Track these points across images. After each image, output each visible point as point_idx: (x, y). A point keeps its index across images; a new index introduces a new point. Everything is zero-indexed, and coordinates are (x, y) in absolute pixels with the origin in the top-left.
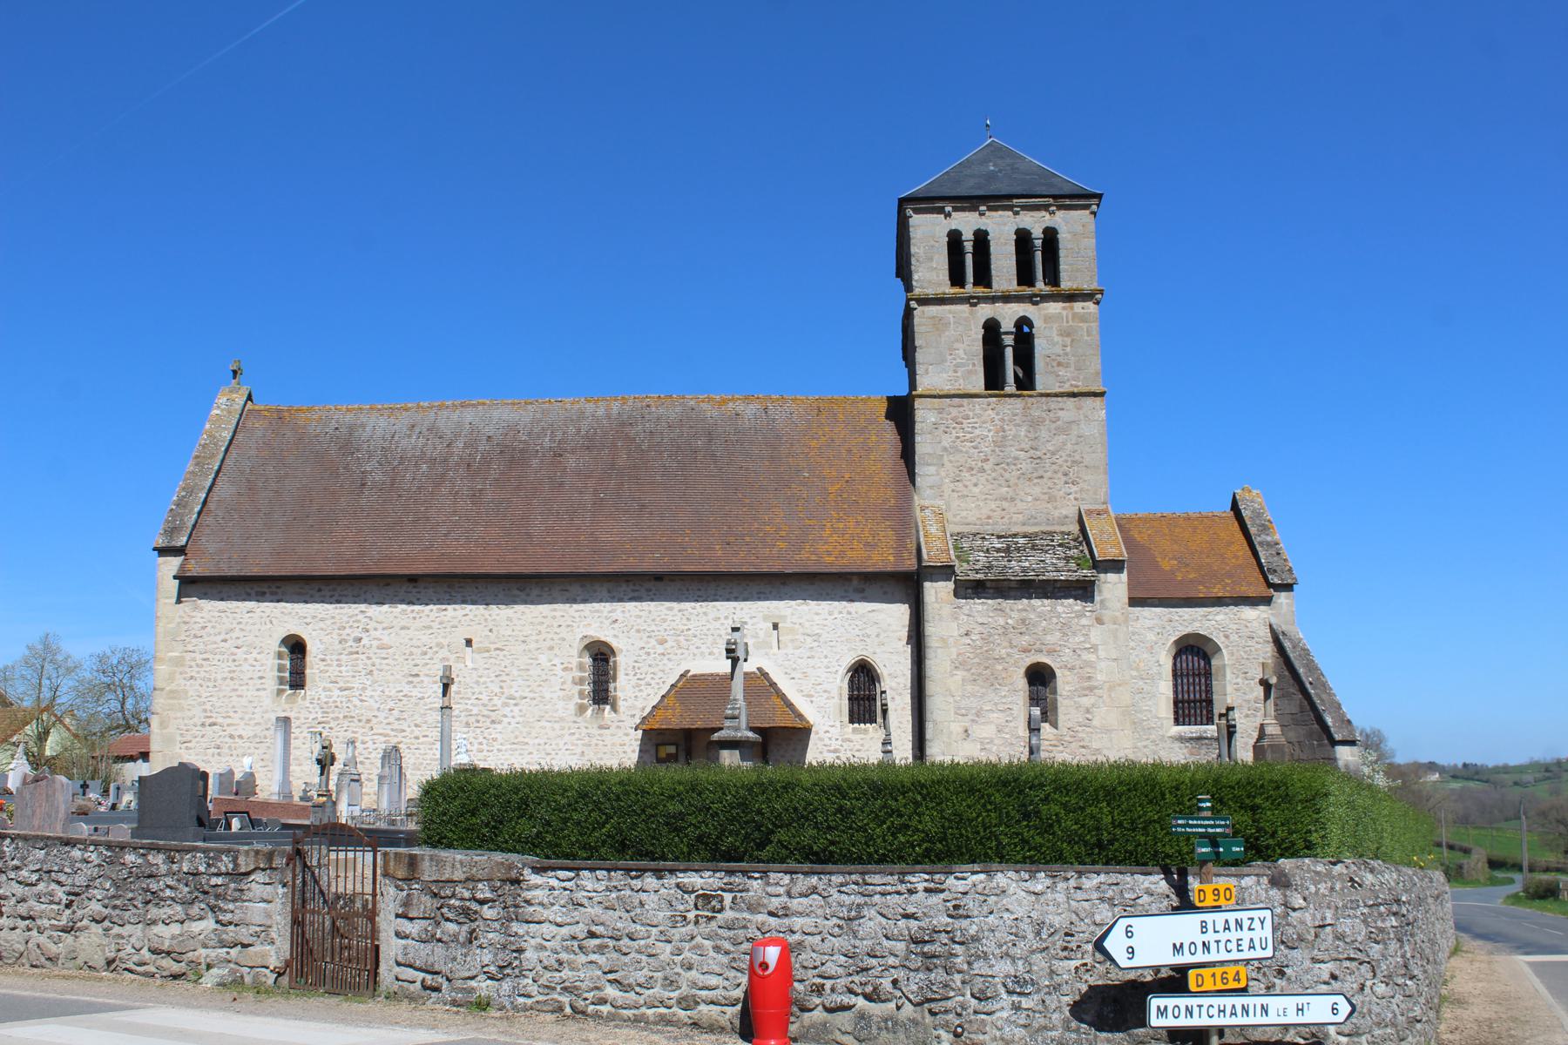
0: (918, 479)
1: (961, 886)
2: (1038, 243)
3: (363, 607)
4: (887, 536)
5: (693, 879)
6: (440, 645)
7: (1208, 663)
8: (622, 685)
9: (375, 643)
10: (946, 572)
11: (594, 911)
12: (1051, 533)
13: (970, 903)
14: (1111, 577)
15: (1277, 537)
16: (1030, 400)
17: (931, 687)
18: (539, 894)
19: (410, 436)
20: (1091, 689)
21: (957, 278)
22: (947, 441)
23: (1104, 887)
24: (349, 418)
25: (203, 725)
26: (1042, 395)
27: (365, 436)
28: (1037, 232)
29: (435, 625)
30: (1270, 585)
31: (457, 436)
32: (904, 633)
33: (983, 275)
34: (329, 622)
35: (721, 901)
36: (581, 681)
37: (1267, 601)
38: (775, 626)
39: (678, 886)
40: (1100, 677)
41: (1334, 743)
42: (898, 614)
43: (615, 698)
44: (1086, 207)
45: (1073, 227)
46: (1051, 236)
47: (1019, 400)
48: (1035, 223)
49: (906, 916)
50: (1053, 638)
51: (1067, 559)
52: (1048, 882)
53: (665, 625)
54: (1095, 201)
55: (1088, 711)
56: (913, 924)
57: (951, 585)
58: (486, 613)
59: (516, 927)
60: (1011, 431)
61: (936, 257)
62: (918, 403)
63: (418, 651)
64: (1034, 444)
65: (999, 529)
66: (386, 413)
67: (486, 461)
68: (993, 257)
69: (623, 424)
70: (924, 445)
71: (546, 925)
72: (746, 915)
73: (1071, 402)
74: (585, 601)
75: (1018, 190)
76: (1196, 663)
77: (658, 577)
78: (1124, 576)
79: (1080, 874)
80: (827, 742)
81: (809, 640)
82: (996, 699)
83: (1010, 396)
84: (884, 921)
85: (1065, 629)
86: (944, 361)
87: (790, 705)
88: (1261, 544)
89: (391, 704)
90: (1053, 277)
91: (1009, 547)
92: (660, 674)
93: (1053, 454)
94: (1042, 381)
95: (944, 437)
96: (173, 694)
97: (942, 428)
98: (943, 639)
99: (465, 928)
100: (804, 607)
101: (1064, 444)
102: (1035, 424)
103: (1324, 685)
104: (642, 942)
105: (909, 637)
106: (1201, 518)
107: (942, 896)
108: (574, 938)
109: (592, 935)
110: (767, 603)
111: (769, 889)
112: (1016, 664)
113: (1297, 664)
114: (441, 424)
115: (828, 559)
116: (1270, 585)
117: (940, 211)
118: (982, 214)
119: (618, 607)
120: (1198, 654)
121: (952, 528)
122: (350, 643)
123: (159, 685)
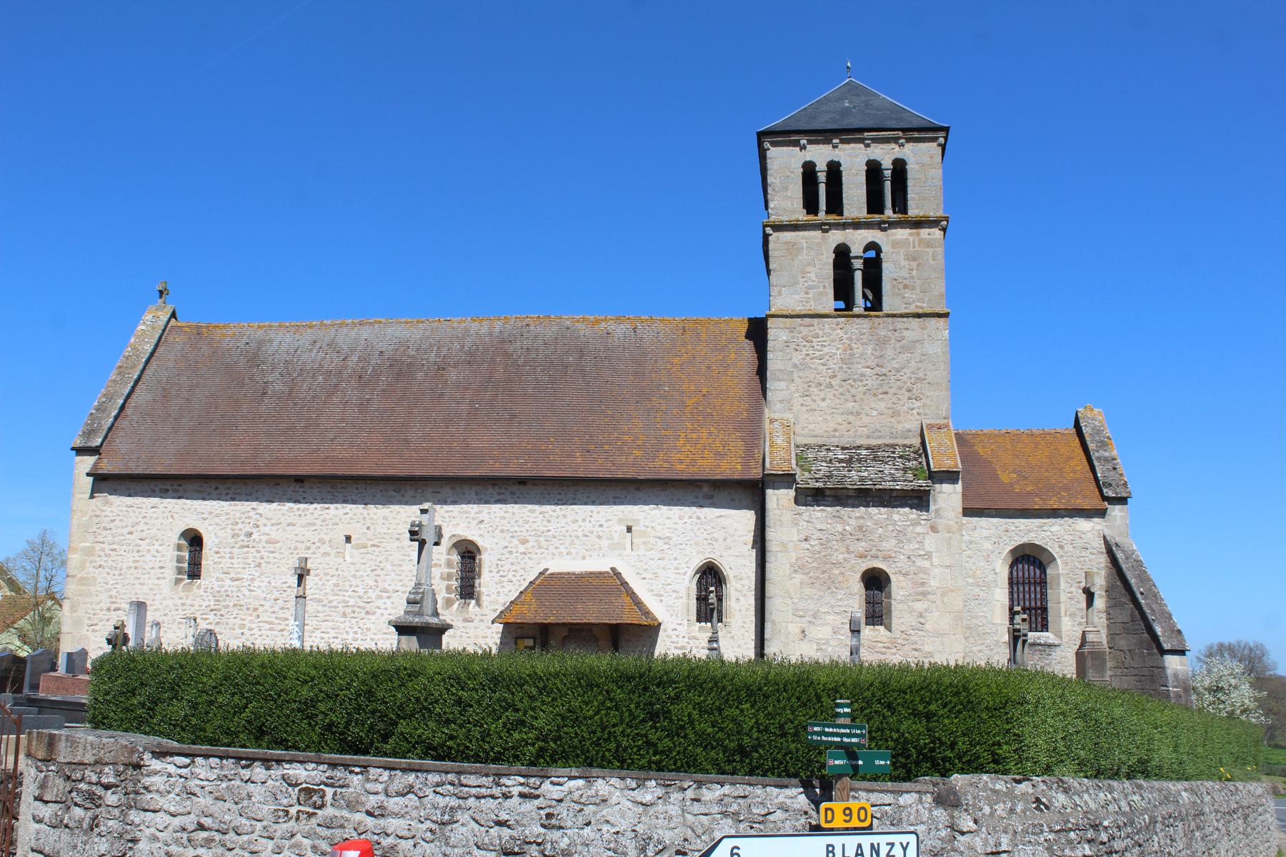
0: (769, 394)
1: (556, 792)
2: (888, 173)
3: (254, 504)
4: (737, 447)
5: (299, 772)
6: (322, 541)
8: (487, 582)
10: (787, 480)
12: (893, 446)
13: (562, 810)
14: (946, 487)
15: (1115, 453)
18: (157, 781)
19: (311, 351)
21: (810, 204)
22: (797, 358)
24: (260, 333)
25: (109, 609)
26: (888, 316)
27: (271, 350)
28: (887, 164)
30: (1105, 498)
31: (352, 351)
33: (835, 205)
34: (223, 518)
35: (323, 797)
36: (449, 577)
37: (1102, 513)
38: (629, 529)
41: (1163, 652)
42: (746, 518)
45: (922, 159)
46: (900, 168)
48: (885, 155)
49: (500, 823)
51: (905, 470)
52: (660, 792)
53: (527, 527)
55: (921, 615)
56: (506, 832)
57: (792, 493)
58: (365, 512)
59: (134, 816)
61: (791, 186)
62: (771, 323)
63: (303, 546)
64: (880, 361)
65: (845, 441)
66: (293, 330)
67: (376, 374)
68: (844, 187)
69: (503, 341)
71: (161, 814)
72: (346, 813)
74: (454, 502)
76: (1035, 572)
77: (522, 481)
79: (700, 784)
81: (660, 543)
84: (476, 826)
85: (900, 535)
86: (796, 283)
87: (638, 603)
88: (1099, 459)
89: (276, 594)
90: (901, 203)
91: (851, 458)
92: (521, 572)
94: (888, 304)
96: (83, 581)
97: (793, 346)
98: (784, 545)
99: (90, 814)
102: (881, 343)
103: (1156, 596)
104: (245, 838)
105: (755, 542)
106: (1045, 435)
107: (536, 802)
109: (201, 827)
110: (622, 507)
111: (369, 786)
113: (1129, 575)
114: (340, 340)
116: (1105, 498)
117: (796, 144)
118: (835, 147)
120: (1033, 564)
121: (802, 440)
122: (242, 537)
123: (71, 572)
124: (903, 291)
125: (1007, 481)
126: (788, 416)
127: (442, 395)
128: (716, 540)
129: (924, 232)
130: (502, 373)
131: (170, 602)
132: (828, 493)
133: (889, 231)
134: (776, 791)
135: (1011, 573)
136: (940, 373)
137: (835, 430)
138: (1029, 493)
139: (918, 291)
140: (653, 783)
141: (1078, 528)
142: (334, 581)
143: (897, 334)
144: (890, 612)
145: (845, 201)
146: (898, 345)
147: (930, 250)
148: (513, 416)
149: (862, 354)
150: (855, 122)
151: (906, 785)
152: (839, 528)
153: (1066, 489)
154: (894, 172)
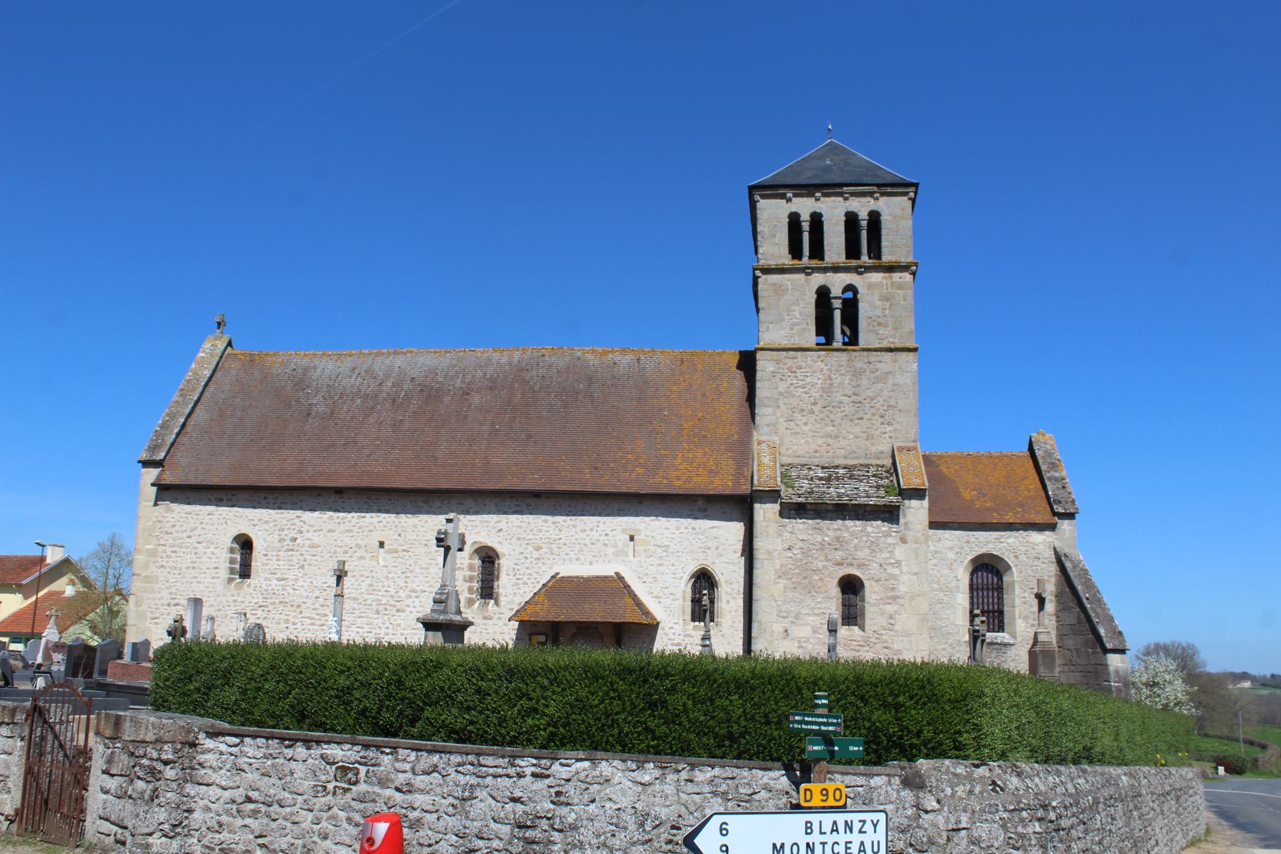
0: (757, 419)
2: (864, 223)
3: (299, 513)
4: (728, 465)
5: (335, 752)
6: (359, 546)
7: (1001, 579)
8: (504, 584)
9: (307, 543)
10: (772, 495)
11: (251, 776)
12: (867, 466)
13: (570, 789)
14: (914, 503)
15: (1064, 473)
18: (210, 758)
19: (350, 377)
21: (795, 251)
22: (782, 387)
23: (717, 781)
25: (169, 605)
26: (864, 350)
28: (863, 215)
29: (355, 529)
30: (1055, 514)
31: (387, 377)
32: (739, 547)
33: (818, 250)
35: (357, 774)
36: (471, 579)
37: (1052, 527)
38: (632, 538)
39: (322, 756)
42: (735, 530)
43: (498, 594)
44: (905, 194)
45: (894, 210)
46: (875, 218)
48: (862, 206)
49: (515, 800)
51: (878, 487)
52: (657, 773)
54: (912, 189)
55: (891, 617)
57: (777, 507)
58: (397, 521)
59: (190, 789)
60: (837, 379)
61: (778, 235)
62: (759, 355)
64: (856, 390)
65: (825, 462)
67: (408, 398)
69: (521, 370)
70: (763, 390)
72: (377, 789)
73: (887, 356)
74: (476, 513)
75: (848, 180)
77: (537, 495)
78: (926, 503)
79: (693, 766)
80: (671, 636)
81: (659, 550)
84: (493, 802)
85: (874, 546)
86: (783, 320)
87: (639, 604)
88: (1050, 479)
89: (317, 593)
90: (875, 250)
91: (830, 476)
92: (535, 575)
93: (872, 399)
94: (865, 339)
95: (781, 383)
96: (148, 579)
97: (779, 376)
98: (769, 553)
99: (151, 786)
100: (656, 523)
101: (881, 391)
102: (858, 374)
103: (1100, 601)
104: (288, 810)
105: (743, 550)
106: (1002, 457)
107: (547, 781)
108: (234, 802)
109: (249, 800)
110: (625, 519)
111: (398, 765)
114: (376, 367)
116: (1055, 514)
117: (783, 196)
118: (817, 200)
119: (503, 518)
120: (992, 571)
121: (786, 460)
123: (137, 572)
126: (776, 438)
127: (466, 417)
129: (896, 276)
130: (518, 397)
131: (222, 599)
132: (809, 507)
134: (761, 773)
135: (971, 580)
136: (909, 401)
138: (987, 509)
140: (652, 765)
141: (1031, 540)
142: (369, 581)
144: (863, 614)
145: (826, 248)
146: (873, 376)
148: (529, 437)
149: (840, 384)
151: (877, 769)
152: (819, 538)
153: (1021, 505)
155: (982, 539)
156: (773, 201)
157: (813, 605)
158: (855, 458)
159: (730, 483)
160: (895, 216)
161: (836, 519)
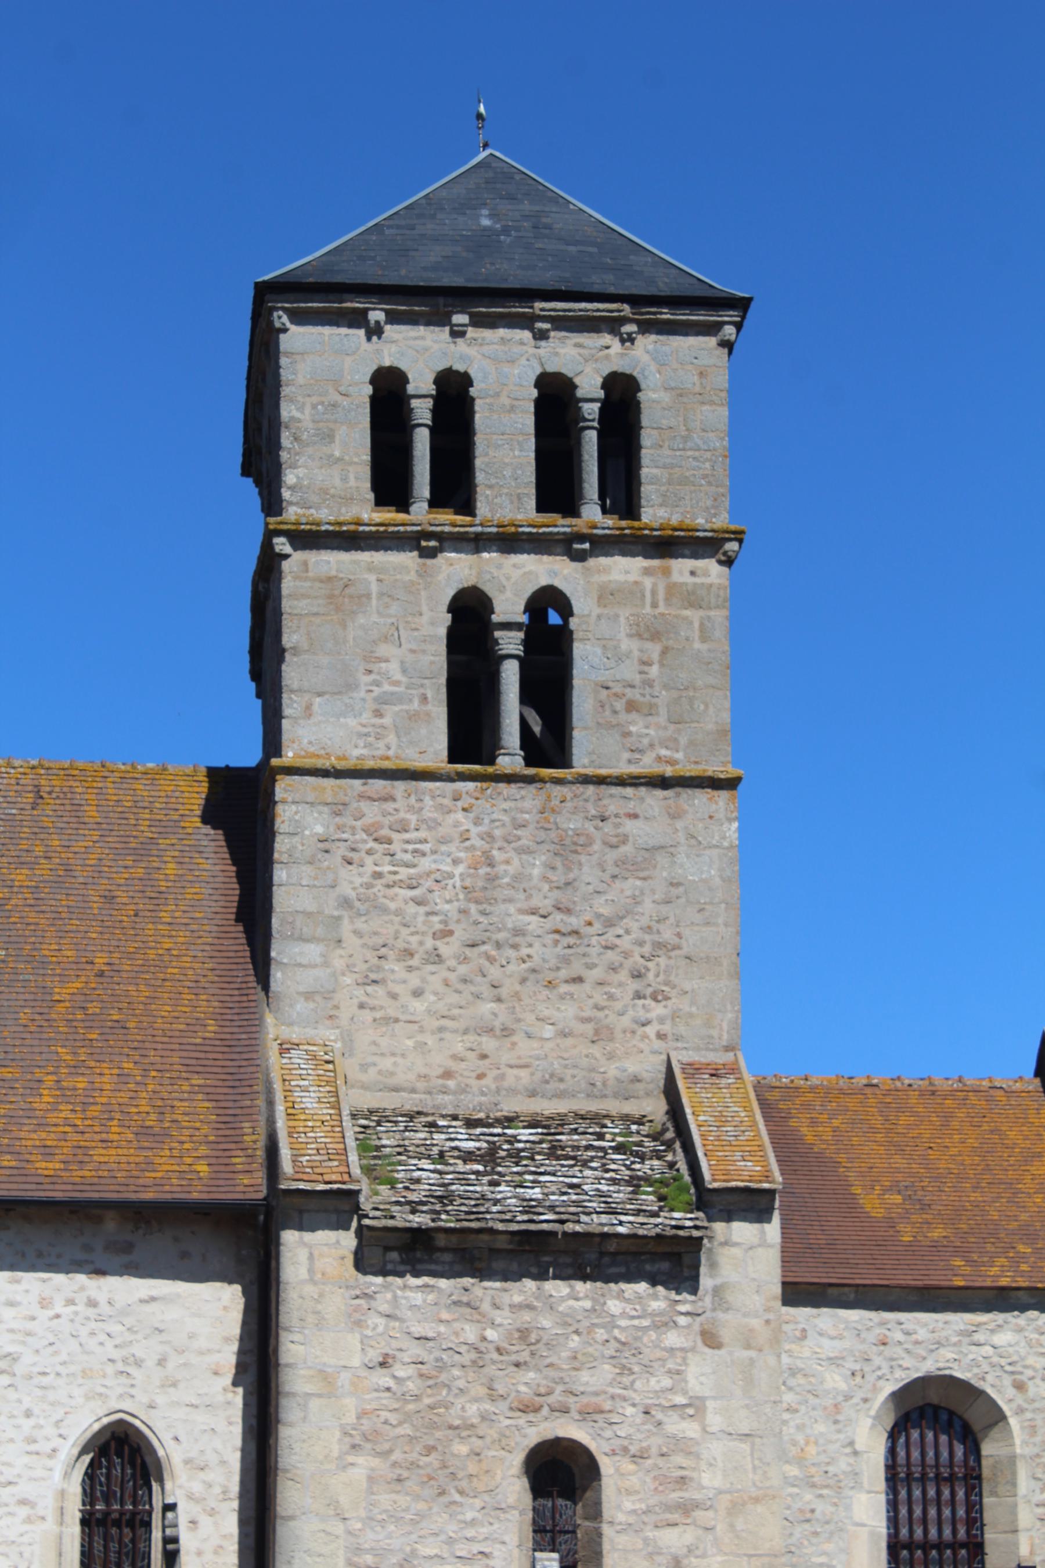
0: (277, 976)
2: (591, 410)
7: (974, 1449)
10: (336, 1206)
12: (597, 1118)
14: (742, 1230)
16: (557, 791)
17: (292, 1497)
20: (687, 1508)
21: (390, 484)
26: (586, 780)
28: (589, 385)
32: (228, 1357)
33: (455, 486)
40: (710, 1480)
45: (677, 374)
46: (622, 395)
47: (532, 789)
48: (586, 361)
50: (596, 1379)
51: (635, 1182)
54: (731, 316)
57: (347, 1240)
61: (341, 432)
62: (284, 788)
65: (472, 1104)
70: (292, 891)
73: (654, 799)
76: (950, 1451)
78: (773, 1229)
82: (451, 1529)
83: (510, 779)
85: (626, 1355)
86: (351, 686)
90: (623, 492)
91: (493, 1148)
93: (609, 923)
94: (588, 747)
98: (326, 1377)
101: (636, 900)
102: (567, 850)
106: (964, 1092)
112: (502, 1442)
115: (45, 1166)
117: (357, 319)
118: (457, 334)
121: (355, 1099)
124: (623, 717)
125: (879, 1213)
126: (328, 1034)
128: (138, 1363)
129: (681, 568)
133: (592, 562)
135: (892, 1452)
136: (715, 933)
137: (447, 1074)
138: (935, 1246)
139: (662, 719)
143: (608, 828)
145: (480, 477)
146: (611, 856)
147: (694, 615)
149: (517, 878)
150: (509, 272)
152: (470, 1333)
153: (1028, 1235)
154: (607, 406)
155: (922, 1334)
156: (327, 330)
157: (451, 1529)
158: (560, 1095)
159: (203, 1168)
160: (680, 393)
161: (517, 1277)
